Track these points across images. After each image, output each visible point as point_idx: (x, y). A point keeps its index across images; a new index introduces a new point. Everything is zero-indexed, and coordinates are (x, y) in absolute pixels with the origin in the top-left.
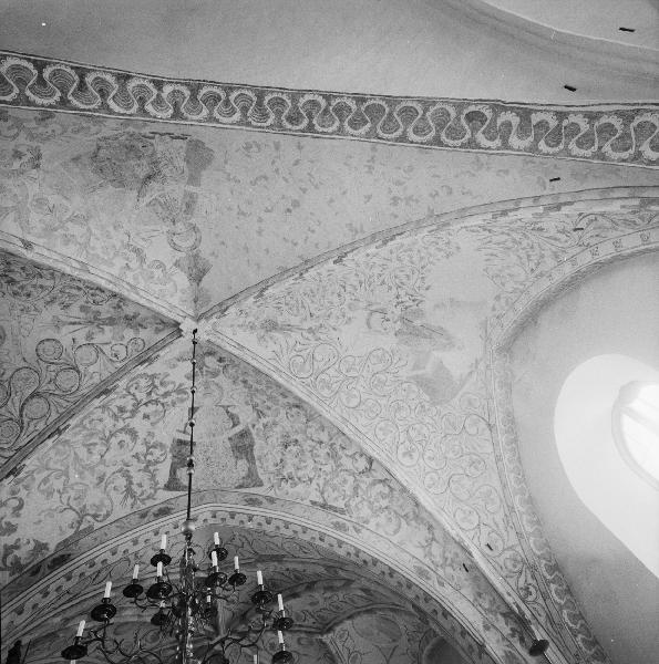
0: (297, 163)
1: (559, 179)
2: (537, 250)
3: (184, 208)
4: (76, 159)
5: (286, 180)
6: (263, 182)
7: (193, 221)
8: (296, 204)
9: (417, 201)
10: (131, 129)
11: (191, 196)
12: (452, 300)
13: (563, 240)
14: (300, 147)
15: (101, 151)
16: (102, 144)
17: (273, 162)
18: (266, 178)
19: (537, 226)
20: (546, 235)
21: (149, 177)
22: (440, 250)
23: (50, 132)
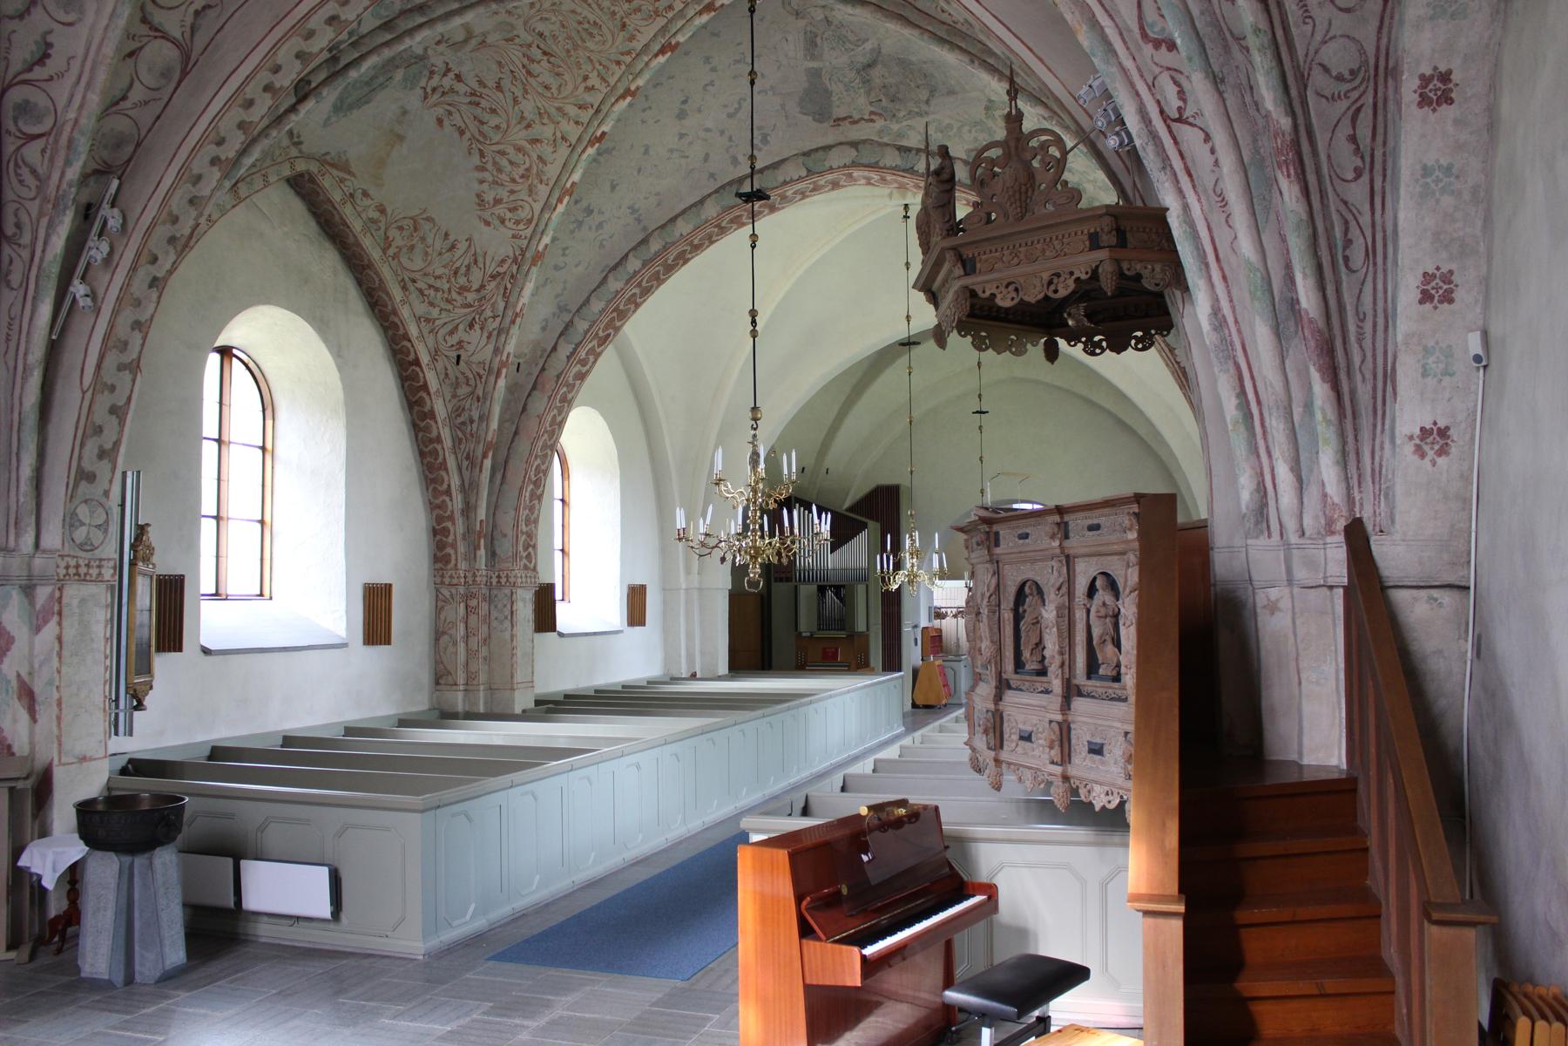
0: (706, 158)
1: (518, 370)
2: (444, 305)
3: (818, 40)
4: (951, 92)
5: (708, 130)
6: (731, 110)
7: (801, 23)
8: (681, 115)
9: (572, 232)
10: (895, 127)
11: (813, 57)
12: (401, 138)
13: (447, 337)
14: (712, 176)
15: (925, 98)
16: (924, 107)
17: (730, 139)
18: (730, 116)
19: (477, 327)
20: (461, 327)
21: (869, 66)
22: (498, 201)
23: (974, 130)
